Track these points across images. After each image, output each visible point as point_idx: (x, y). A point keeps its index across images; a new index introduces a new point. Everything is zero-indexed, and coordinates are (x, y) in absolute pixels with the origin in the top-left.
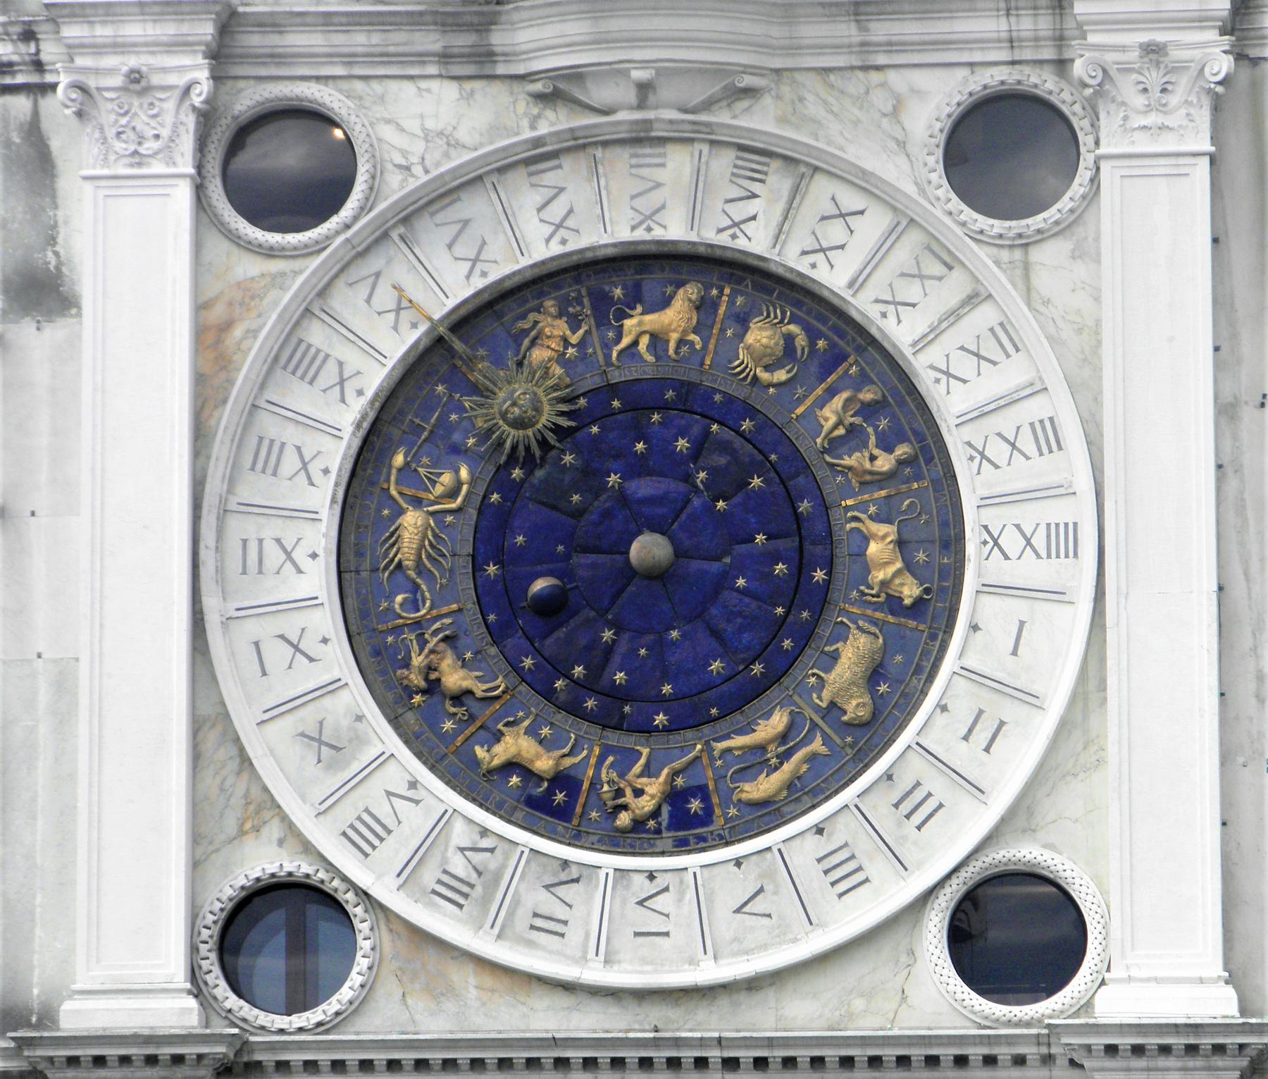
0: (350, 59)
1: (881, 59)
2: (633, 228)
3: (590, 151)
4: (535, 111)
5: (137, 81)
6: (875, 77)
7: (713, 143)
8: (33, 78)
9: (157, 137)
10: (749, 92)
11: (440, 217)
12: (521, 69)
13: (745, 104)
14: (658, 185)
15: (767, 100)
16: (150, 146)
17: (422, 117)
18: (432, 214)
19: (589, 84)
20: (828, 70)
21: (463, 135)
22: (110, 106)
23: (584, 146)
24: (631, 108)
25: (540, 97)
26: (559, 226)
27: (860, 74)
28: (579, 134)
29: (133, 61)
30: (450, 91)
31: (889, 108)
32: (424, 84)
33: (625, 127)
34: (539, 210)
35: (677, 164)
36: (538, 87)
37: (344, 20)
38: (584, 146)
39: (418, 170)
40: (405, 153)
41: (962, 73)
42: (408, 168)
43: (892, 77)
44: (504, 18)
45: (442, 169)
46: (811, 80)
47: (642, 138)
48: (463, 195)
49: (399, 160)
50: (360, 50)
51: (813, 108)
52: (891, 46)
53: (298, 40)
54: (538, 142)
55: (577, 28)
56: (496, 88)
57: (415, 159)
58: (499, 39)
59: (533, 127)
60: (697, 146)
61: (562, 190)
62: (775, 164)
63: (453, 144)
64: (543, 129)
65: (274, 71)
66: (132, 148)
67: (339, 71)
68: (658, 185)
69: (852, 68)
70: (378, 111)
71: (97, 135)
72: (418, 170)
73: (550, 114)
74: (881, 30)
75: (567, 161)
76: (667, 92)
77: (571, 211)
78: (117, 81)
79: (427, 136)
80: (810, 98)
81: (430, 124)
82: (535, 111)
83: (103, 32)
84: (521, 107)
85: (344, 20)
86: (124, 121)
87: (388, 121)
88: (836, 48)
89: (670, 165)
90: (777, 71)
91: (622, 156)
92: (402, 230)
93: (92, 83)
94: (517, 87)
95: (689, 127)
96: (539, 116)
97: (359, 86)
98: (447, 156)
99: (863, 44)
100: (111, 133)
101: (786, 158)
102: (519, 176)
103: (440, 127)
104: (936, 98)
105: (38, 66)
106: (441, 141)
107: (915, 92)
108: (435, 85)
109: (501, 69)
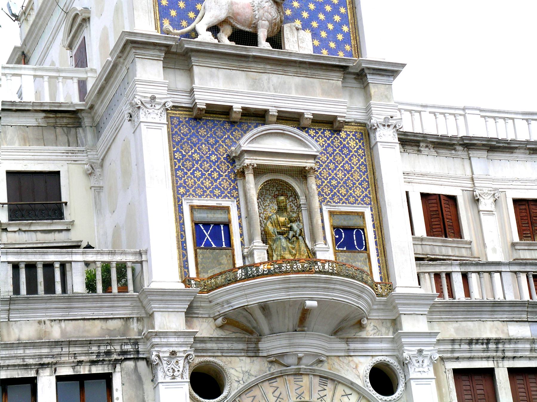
0: (222, 350)
1: (352, 354)
2: (297, 398)
3: (284, 377)
4: (270, 366)
5: (173, 354)
6: (350, 358)
7: (314, 375)
8: (136, 356)
9: (179, 371)
10: (321, 361)
11: (248, 395)
12: (265, 354)
13: (320, 365)
14: (302, 386)
15: (326, 364)
16: (176, 373)
17: (241, 367)
18: (246, 395)
19: (285, 358)
20: (339, 356)
21: (252, 372)
22: (165, 362)
23: (282, 376)
24: (295, 365)
25: (271, 362)
26: (278, 398)
27: (347, 358)
28: (283, 372)
29: (171, 349)
30: (248, 360)
31: (355, 367)
32: (241, 358)
33: (293, 370)
34: (273, 393)
35: (306, 380)
36: (272, 359)
37: (222, 339)
38: (282, 376)
39: (241, 382)
40: (238, 377)
41: (370, 358)
42: (239, 381)
43: (354, 358)
44: (263, 340)
45: (250, 381)
46: (336, 359)
47: (298, 374)
48: (253, 389)
49: (237, 379)
50: (225, 348)
51: (337, 366)
52: (355, 350)
53: (209, 346)
54: (273, 374)
55: (284, 342)
56: (259, 358)
57: (241, 379)
58: (261, 345)
59: (269, 371)
60: (310, 376)
61: (278, 388)
62: (329, 382)
63: (250, 375)
64: (272, 371)
65: (202, 354)
66: (172, 374)
67: (220, 354)
68: (302, 386)
69: (345, 356)
70: (230, 366)
71: (162, 370)
72: (241, 382)
73: (273, 366)
74: (352, 346)
75: (278, 379)
76: (304, 361)
77: (281, 394)
78: (168, 355)
79: (244, 373)
80: (336, 363)
81: (244, 369)
82: (270, 366)
83: (164, 340)
84: (266, 364)
85: (222, 339)
86: (169, 366)
87: (233, 368)
88: (341, 350)
89: (304, 381)
90: (327, 356)
91: (292, 378)
92: (239, 399)
93: (161, 355)
94: (265, 359)
95: (309, 370)
96: (270, 368)
97: (224, 358)
98: (249, 378)
99: (349, 349)
100: (166, 369)
101: (332, 380)
102: (267, 383)
103: (247, 370)
104: (365, 365)
105: (138, 352)
106: (247, 374)
107: (360, 363)
108: (244, 358)
109: (261, 354)
